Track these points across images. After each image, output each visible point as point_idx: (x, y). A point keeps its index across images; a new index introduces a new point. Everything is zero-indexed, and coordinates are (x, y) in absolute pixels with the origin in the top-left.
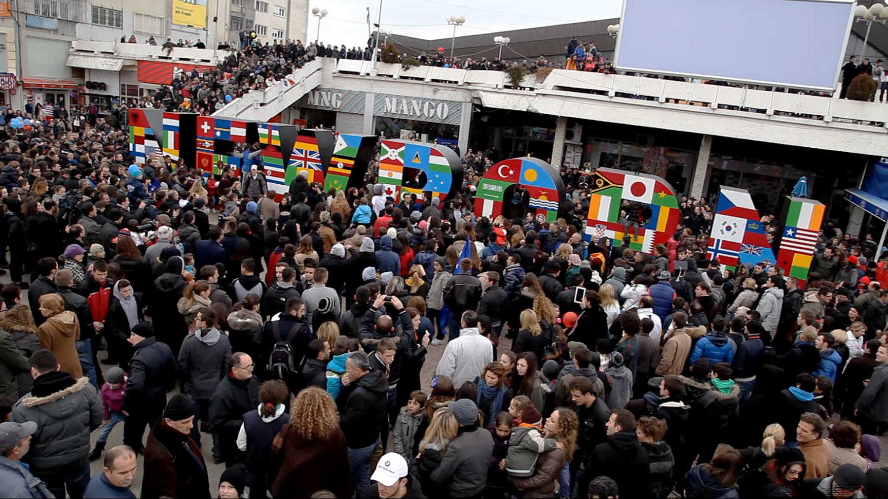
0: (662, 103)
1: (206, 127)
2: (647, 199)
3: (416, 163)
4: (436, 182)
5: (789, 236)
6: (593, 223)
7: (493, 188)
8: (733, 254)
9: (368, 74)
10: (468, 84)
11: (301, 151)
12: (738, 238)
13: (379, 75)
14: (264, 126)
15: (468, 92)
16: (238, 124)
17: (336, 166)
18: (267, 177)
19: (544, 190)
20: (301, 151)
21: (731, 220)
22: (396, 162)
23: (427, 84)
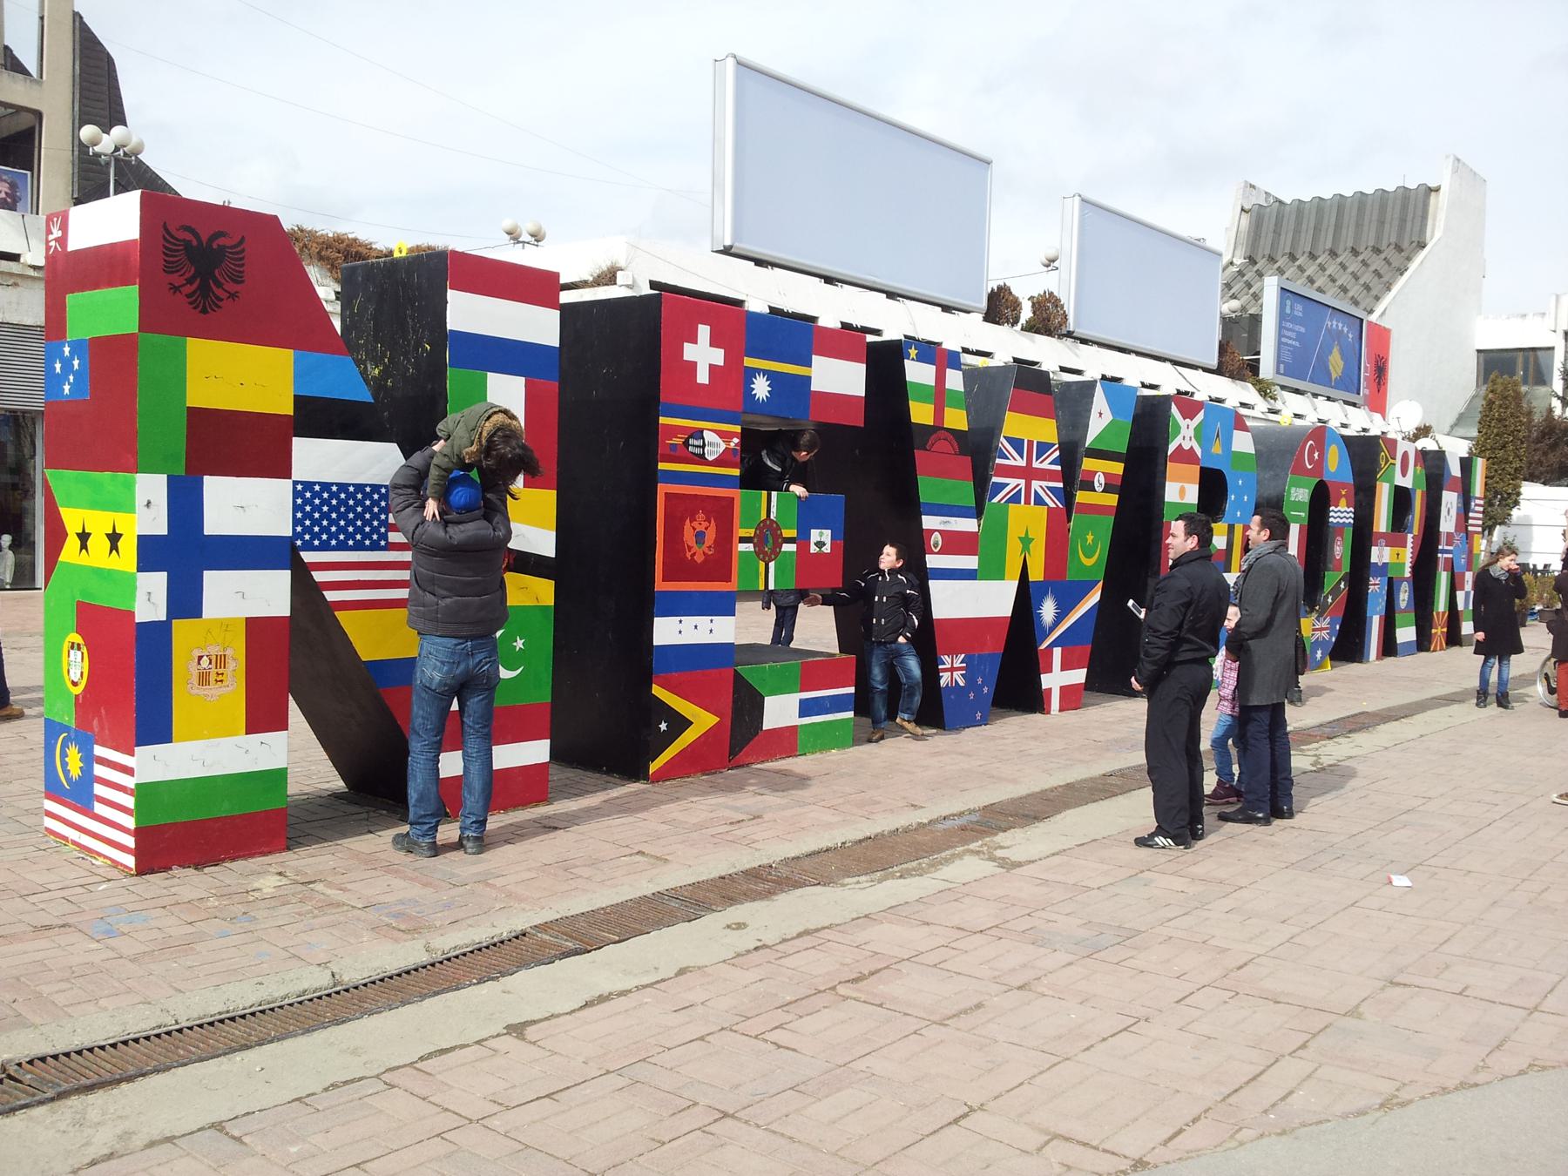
1: (703, 354)
20: (1017, 444)
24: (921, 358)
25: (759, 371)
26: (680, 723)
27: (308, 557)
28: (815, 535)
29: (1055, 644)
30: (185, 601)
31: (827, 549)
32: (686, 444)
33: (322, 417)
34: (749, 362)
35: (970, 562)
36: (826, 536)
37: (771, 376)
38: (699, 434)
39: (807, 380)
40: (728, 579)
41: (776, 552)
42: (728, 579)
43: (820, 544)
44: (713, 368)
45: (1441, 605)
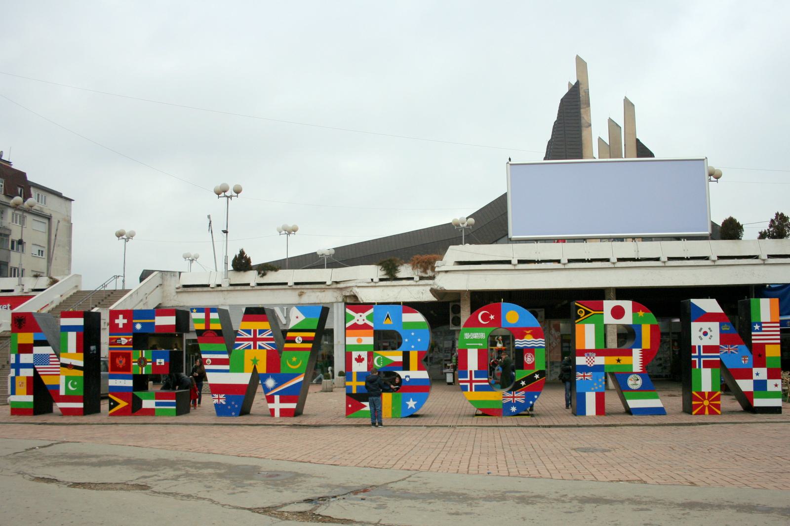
0: (564, 264)
2: (628, 319)
3: (388, 324)
4: (413, 340)
5: (757, 331)
6: (582, 353)
7: (475, 336)
8: (714, 357)
9: (219, 286)
10: (337, 283)
11: (249, 332)
12: (715, 341)
13: (231, 285)
14: (199, 310)
15: (338, 292)
17: (294, 342)
18: (206, 367)
19: (528, 329)
20: (249, 332)
21: (705, 326)
22: (365, 327)
23: (291, 288)
24: (197, 312)
25: (138, 323)
27: (36, 366)
28: (158, 361)
29: (277, 393)
30: (17, 373)
31: (163, 364)
32: (116, 341)
34: (134, 321)
35: (227, 367)
36: (163, 361)
38: (120, 339)
39: (154, 323)
41: (145, 365)
43: (160, 363)
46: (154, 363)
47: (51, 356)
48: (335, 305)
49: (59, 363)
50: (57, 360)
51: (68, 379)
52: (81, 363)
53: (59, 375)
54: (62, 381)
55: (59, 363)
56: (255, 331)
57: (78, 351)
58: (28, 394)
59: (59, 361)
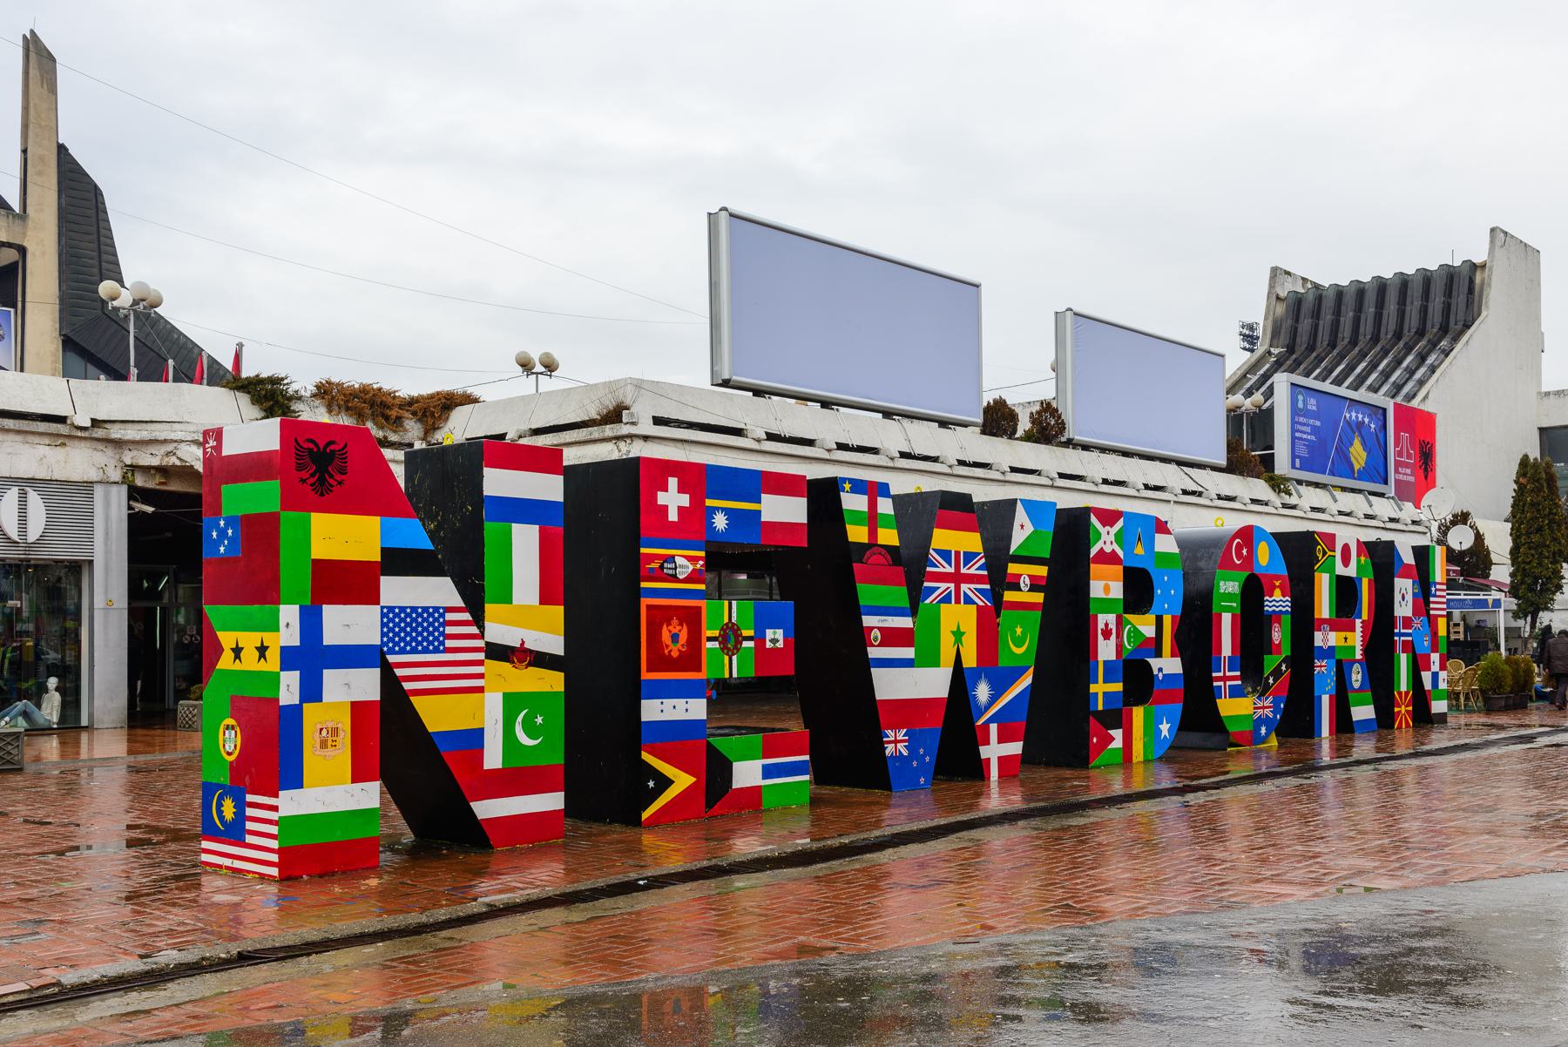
1: (673, 499)
15: (110, 451)
16: (783, 485)
20: (945, 554)
24: (853, 491)
25: (718, 509)
26: (665, 783)
27: (392, 658)
28: (770, 634)
29: (991, 720)
30: (312, 691)
31: (780, 645)
32: (662, 567)
33: (399, 561)
34: (709, 503)
35: (908, 653)
37: (727, 511)
38: (672, 559)
40: (699, 669)
41: (737, 648)
42: (699, 669)
43: (774, 641)
44: (681, 509)
45: (1403, 683)
46: (759, 640)
47: (450, 616)
48: (99, 491)
49: (480, 643)
50: (474, 630)
51: (513, 703)
52: (554, 644)
53: (480, 690)
54: (489, 713)
55: (480, 643)
56: (958, 553)
57: (546, 598)
58: (359, 774)
59: (482, 636)
